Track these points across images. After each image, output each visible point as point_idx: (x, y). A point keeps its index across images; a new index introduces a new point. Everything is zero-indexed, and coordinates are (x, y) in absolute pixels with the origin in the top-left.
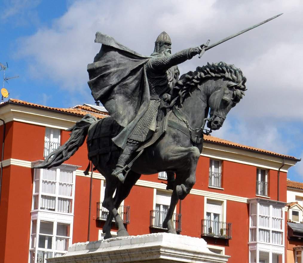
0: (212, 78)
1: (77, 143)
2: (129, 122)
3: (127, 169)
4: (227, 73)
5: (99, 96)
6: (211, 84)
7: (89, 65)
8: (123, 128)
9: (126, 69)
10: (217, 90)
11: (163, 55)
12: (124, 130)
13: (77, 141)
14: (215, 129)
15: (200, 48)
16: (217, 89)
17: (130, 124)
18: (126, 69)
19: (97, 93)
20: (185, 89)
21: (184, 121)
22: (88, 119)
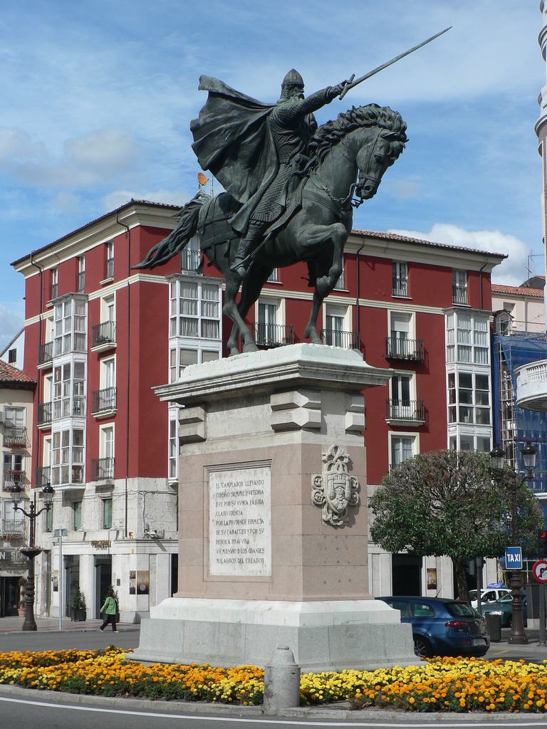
0: (360, 126)
1: (187, 232)
2: (250, 196)
3: (250, 260)
4: (379, 118)
5: (207, 163)
6: (359, 134)
7: (192, 122)
8: (242, 204)
9: (243, 124)
10: (368, 143)
11: (293, 101)
12: (243, 208)
13: (185, 230)
14: (367, 198)
15: (341, 86)
16: (367, 141)
17: (251, 199)
18: (243, 124)
19: (206, 159)
20: (325, 145)
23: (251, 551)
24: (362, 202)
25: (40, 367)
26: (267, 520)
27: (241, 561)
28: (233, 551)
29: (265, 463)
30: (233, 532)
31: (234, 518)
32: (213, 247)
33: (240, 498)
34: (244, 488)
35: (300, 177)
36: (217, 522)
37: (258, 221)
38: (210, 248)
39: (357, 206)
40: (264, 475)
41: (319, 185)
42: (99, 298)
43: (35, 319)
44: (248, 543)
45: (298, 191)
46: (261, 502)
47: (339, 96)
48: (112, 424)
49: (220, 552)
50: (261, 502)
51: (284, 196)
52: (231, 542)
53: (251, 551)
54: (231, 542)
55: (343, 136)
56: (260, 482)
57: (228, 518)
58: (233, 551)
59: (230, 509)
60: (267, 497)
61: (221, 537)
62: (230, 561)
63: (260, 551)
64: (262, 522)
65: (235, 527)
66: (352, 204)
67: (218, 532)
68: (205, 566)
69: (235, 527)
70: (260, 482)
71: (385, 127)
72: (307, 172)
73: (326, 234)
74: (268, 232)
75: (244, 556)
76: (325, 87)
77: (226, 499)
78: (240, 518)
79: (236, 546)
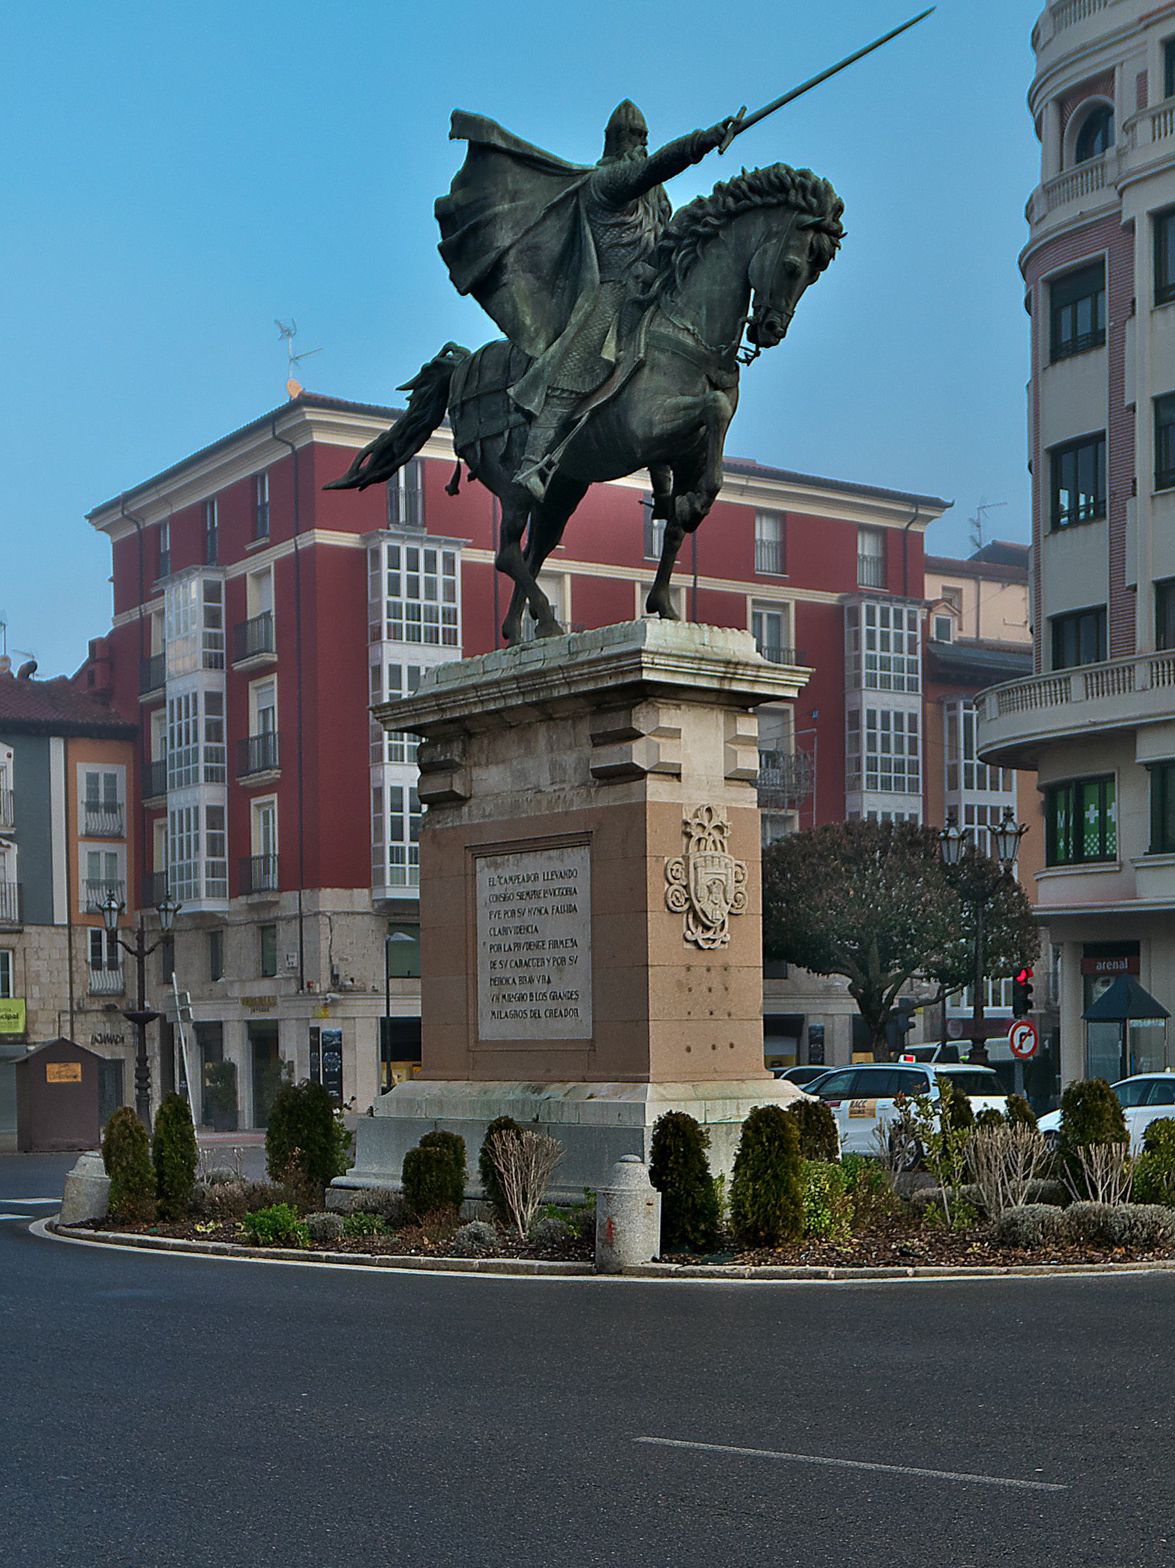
4: (793, 192)
15: (722, 130)
17: (551, 349)
21: (688, 330)
23: (555, 996)
24: (757, 354)
25: (143, 699)
26: (584, 940)
27: (536, 1015)
28: (522, 998)
30: (519, 964)
31: (522, 939)
33: (534, 904)
34: (540, 885)
36: (492, 947)
38: (472, 445)
39: (748, 362)
40: (578, 859)
42: (245, 575)
43: (135, 614)
44: (549, 982)
47: (717, 148)
48: (274, 797)
53: (555, 996)
56: (570, 874)
57: (511, 938)
58: (522, 998)
59: (517, 922)
60: (582, 900)
61: (499, 973)
62: (516, 1015)
65: (525, 955)
66: (737, 358)
68: (470, 1024)
69: (525, 955)
70: (570, 874)
72: (656, 297)
75: (542, 1007)
76: (690, 132)
77: (509, 906)
78: (533, 938)
79: (525, 990)
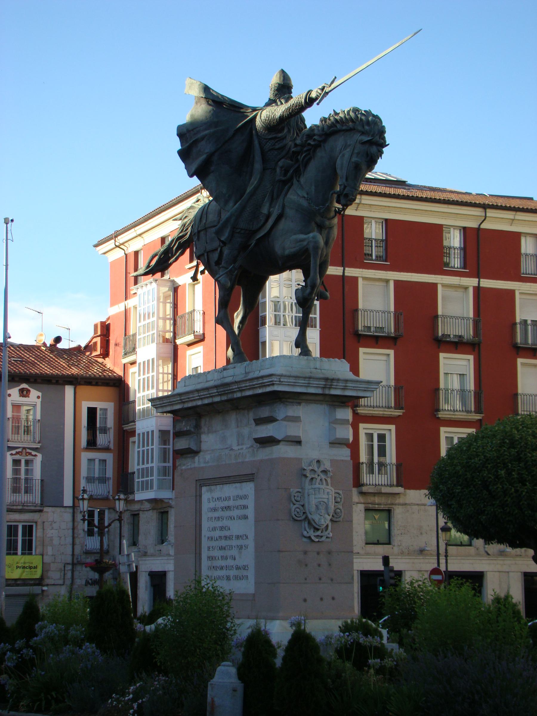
21: (305, 197)
22: (199, 202)
26: (251, 535)
28: (222, 568)
29: (249, 478)
30: (222, 548)
32: (206, 254)
34: (231, 503)
35: (284, 183)
37: (242, 229)
40: (248, 488)
41: (299, 192)
44: (235, 559)
45: (281, 200)
46: (246, 517)
49: (211, 568)
50: (246, 517)
51: (267, 205)
52: (220, 558)
54: (220, 558)
55: (325, 141)
57: (217, 533)
58: (222, 568)
60: (250, 512)
63: (245, 568)
64: (247, 537)
65: (223, 543)
67: (209, 548)
69: (223, 543)
70: (245, 497)
71: (363, 133)
73: (305, 243)
74: (253, 242)
78: (227, 533)
